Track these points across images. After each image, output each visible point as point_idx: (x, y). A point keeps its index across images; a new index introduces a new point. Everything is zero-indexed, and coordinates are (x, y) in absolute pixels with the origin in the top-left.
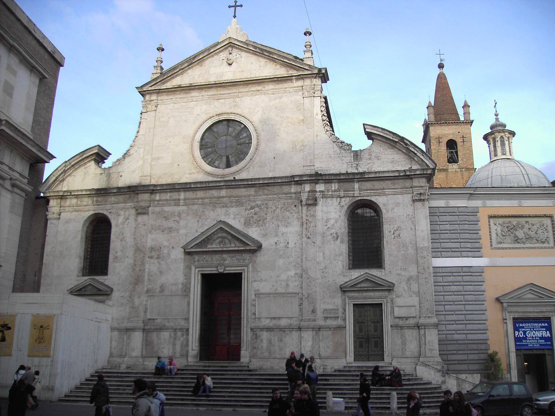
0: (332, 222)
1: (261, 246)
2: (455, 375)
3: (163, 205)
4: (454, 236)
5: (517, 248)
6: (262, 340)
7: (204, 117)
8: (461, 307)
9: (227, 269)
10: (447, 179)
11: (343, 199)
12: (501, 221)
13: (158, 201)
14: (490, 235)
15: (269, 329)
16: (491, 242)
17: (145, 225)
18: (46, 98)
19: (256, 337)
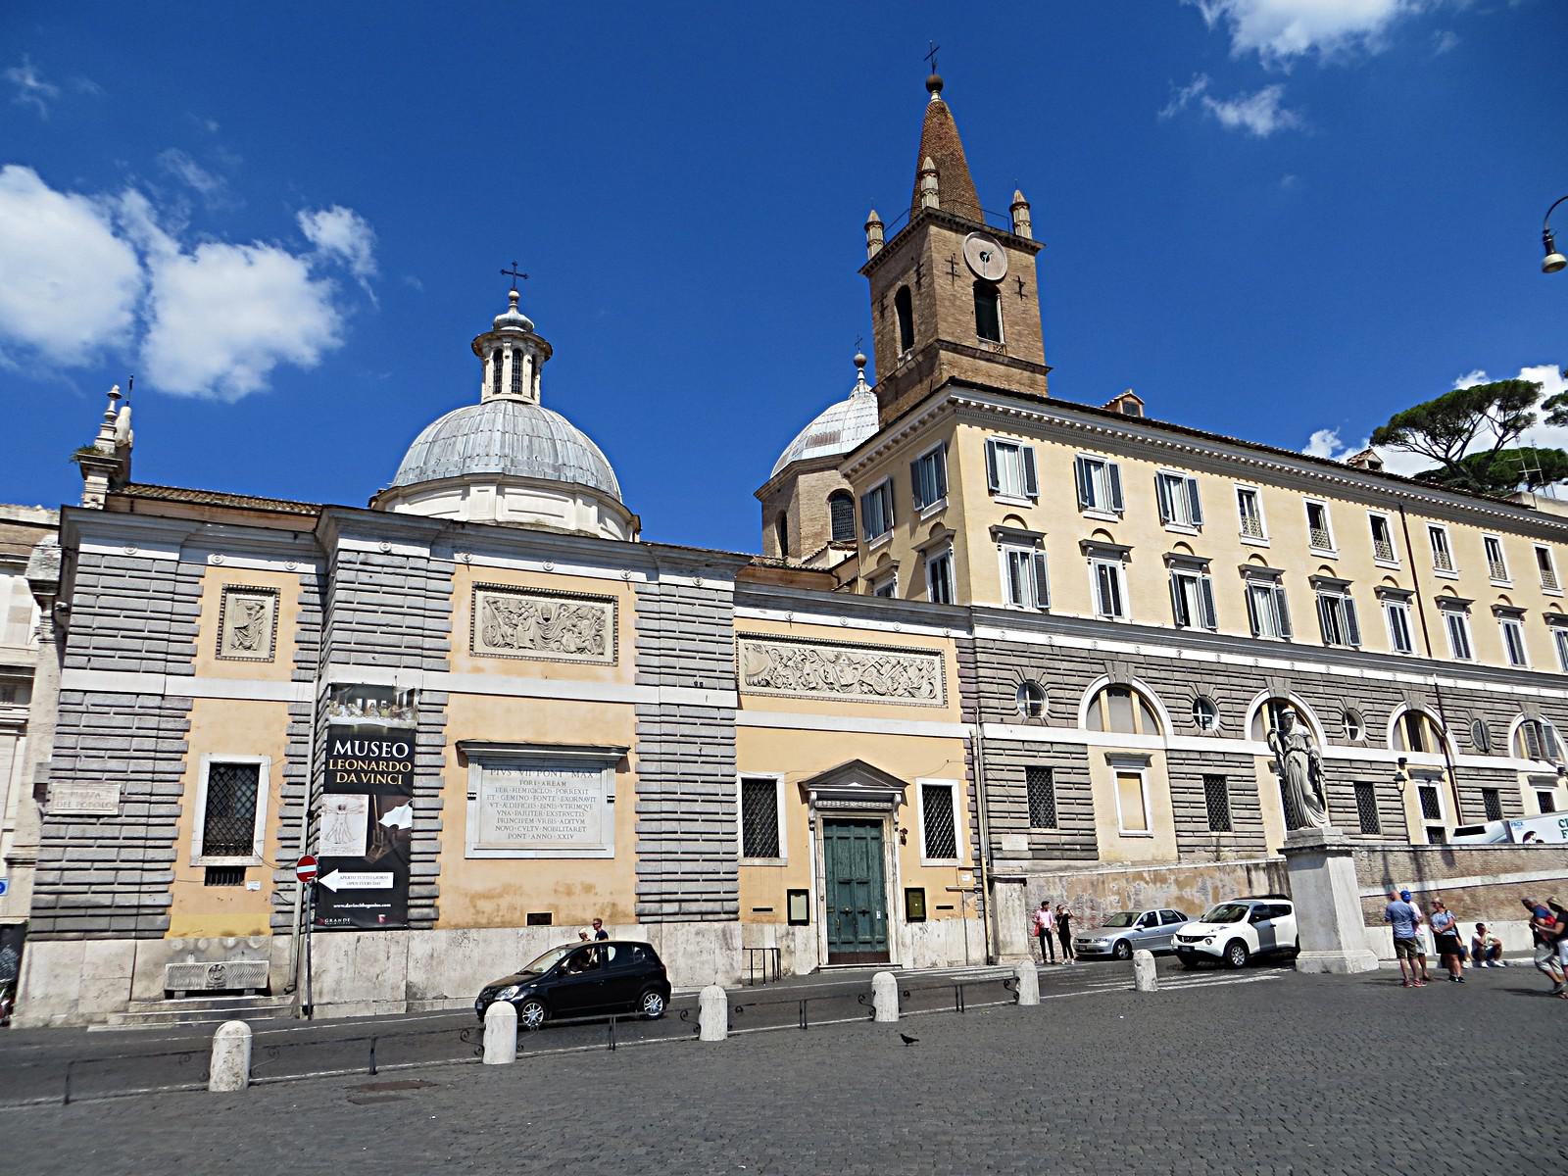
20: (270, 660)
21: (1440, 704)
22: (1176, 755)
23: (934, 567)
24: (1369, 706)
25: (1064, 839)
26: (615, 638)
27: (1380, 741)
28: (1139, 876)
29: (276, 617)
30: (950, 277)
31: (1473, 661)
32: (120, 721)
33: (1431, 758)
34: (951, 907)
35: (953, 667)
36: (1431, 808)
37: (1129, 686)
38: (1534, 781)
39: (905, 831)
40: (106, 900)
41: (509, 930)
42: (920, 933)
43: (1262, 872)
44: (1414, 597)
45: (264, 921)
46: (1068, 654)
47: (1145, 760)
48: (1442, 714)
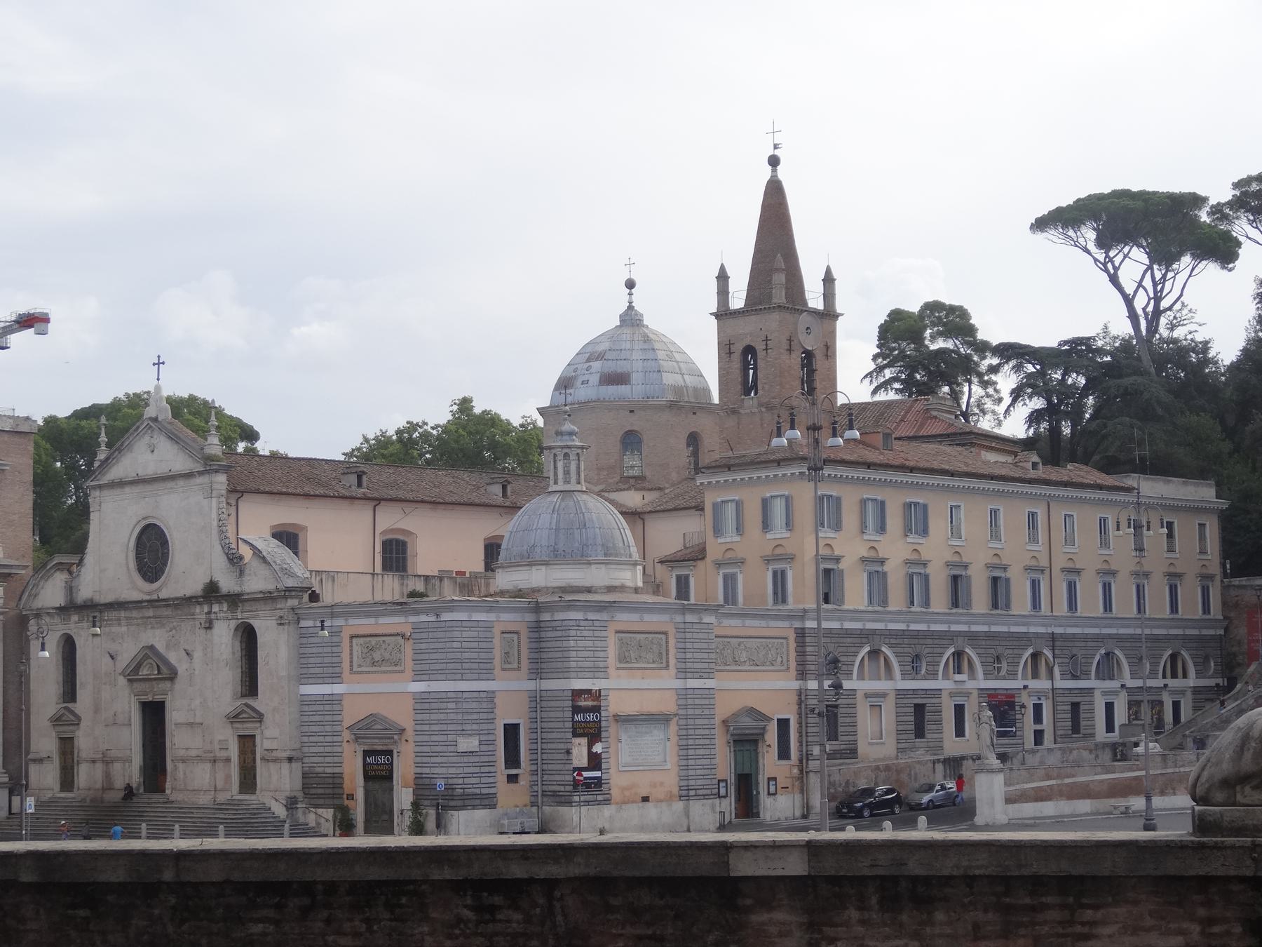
0: (224, 646)
1: (176, 674)
2: (313, 810)
3: (110, 625)
4: (319, 660)
5: (372, 672)
6: (179, 772)
7: (134, 521)
8: (321, 739)
9: (156, 697)
10: (739, 428)
11: (231, 621)
12: (362, 640)
13: (107, 621)
14: (351, 658)
15: (184, 761)
16: (351, 666)
17: (98, 648)
18: (17, 488)
19: (176, 768)
20: (519, 669)
21: (1053, 646)
22: (901, 693)
23: (775, 573)
24: (1011, 651)
25: (843, 747)
26: (667, 654)
27: (1012, 675)
28: (877, 768)
29: (519, 646)
30: (789, 352)
31: (1078, 614)
32: (474, 705)
33: (1043, 684)
34: (788, 788)
35: (793, 645)
36: (1038, 718)
37: (879, 650)
38: (1105, 693)
39: (769, 746)
40: (478, 791)
41: (635, 804)
42: (774, 802)
43: (941, 764)
44: (1047, 572)
45: (527, 799)
46: (848, 633)
47: (883, 695)
48: (1054, 653)
